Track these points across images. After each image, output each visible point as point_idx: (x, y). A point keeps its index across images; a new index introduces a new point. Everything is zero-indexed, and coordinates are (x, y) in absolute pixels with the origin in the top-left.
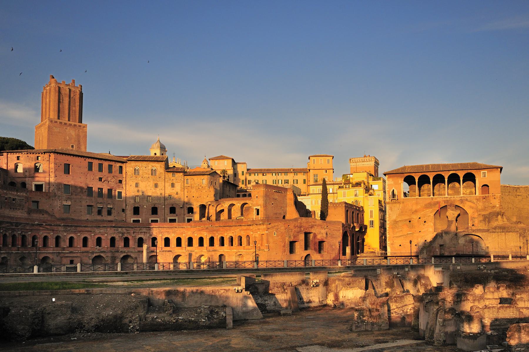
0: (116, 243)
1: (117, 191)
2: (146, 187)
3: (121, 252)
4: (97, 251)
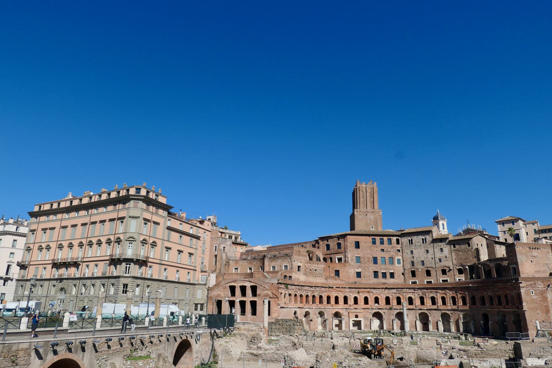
0: (391, 301)
4: (375, 307)
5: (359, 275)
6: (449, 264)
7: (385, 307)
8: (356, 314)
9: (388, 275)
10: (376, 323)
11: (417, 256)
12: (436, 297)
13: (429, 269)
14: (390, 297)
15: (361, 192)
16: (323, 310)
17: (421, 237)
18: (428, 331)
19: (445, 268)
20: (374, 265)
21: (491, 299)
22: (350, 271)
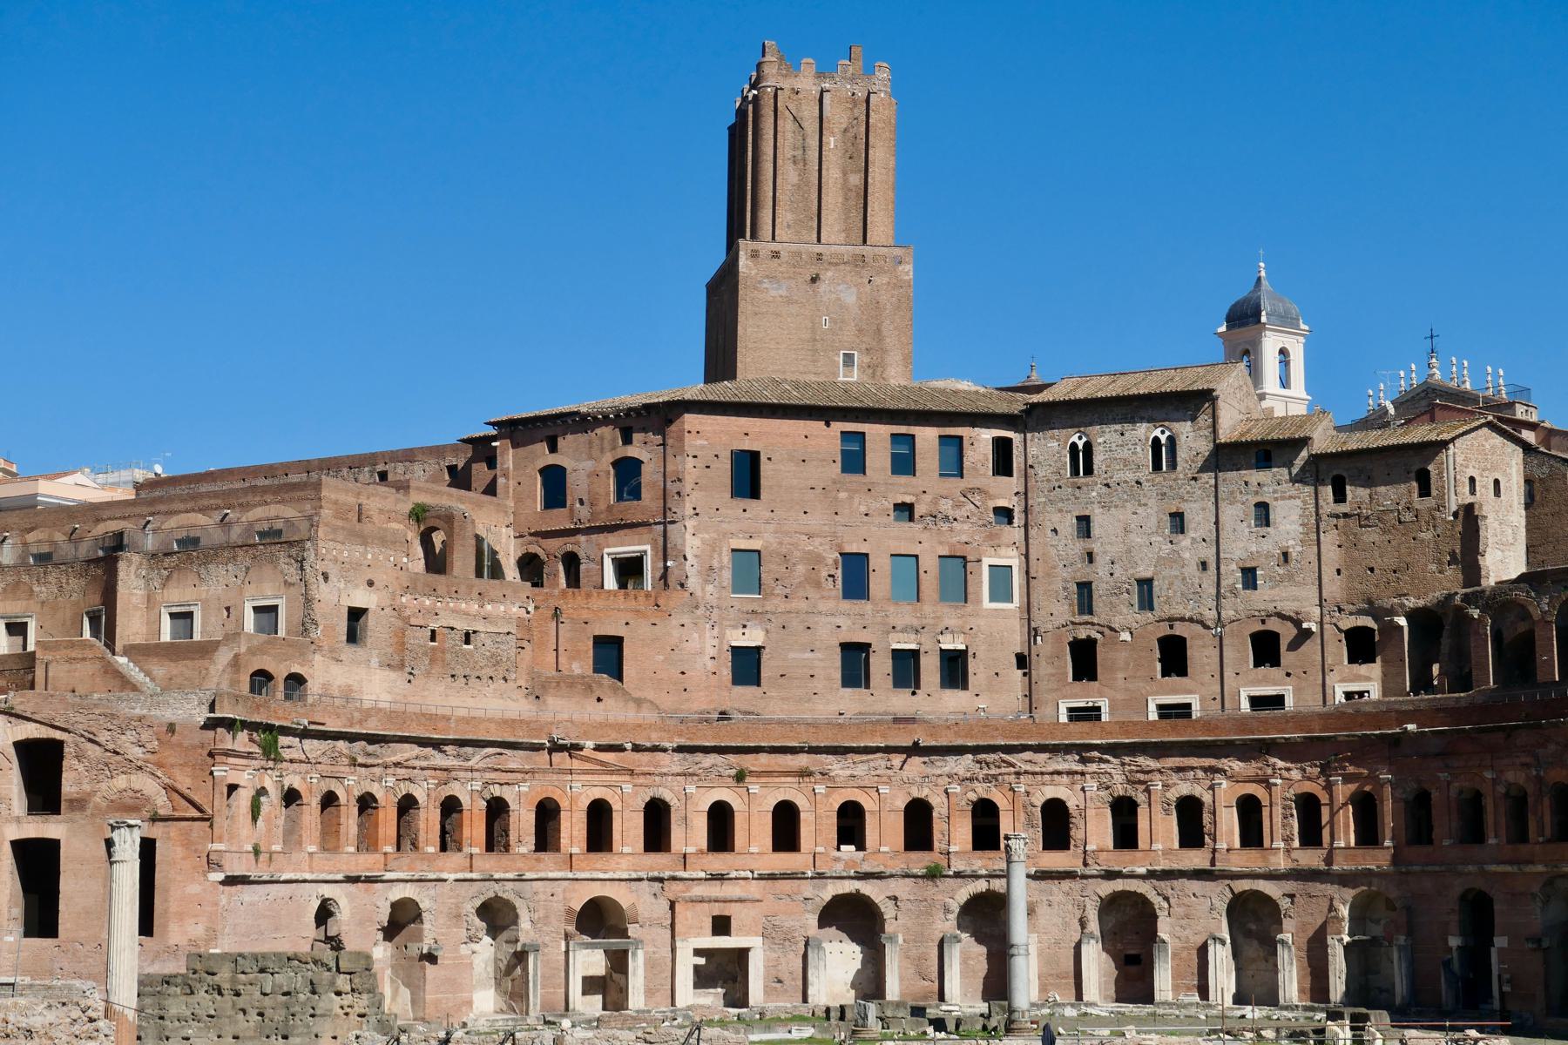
0: (938, 827)
1: (987, 562)
2: (1126, 531)
3: (958, 875)
4: (839, 869)
5: (747, 665)
6: (1299, 598)
7: (897, 866)
8: (718, 910)
9: (930, 668)
10: (840, 962)
11: (1114, 550)
12: (1207, 798)
13: (1180, 630)
14: (937, 802)
15: (787, 125)
16: (507, 892)
17: (1145, 432)
18: (1148, 998)
19: (1273, 625)
20: (847, 605)
21: (1519, 805)
22: (694, 645)
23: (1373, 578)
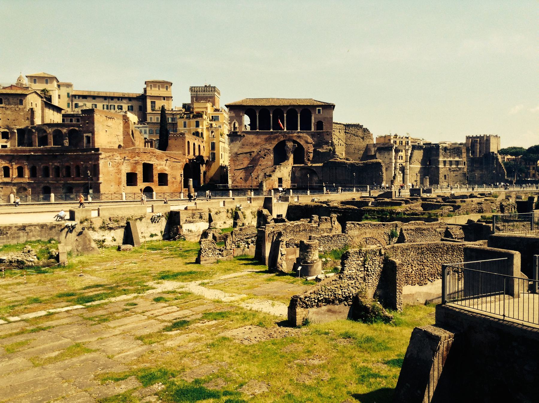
21: (57, 170)
23: (9, 121)
